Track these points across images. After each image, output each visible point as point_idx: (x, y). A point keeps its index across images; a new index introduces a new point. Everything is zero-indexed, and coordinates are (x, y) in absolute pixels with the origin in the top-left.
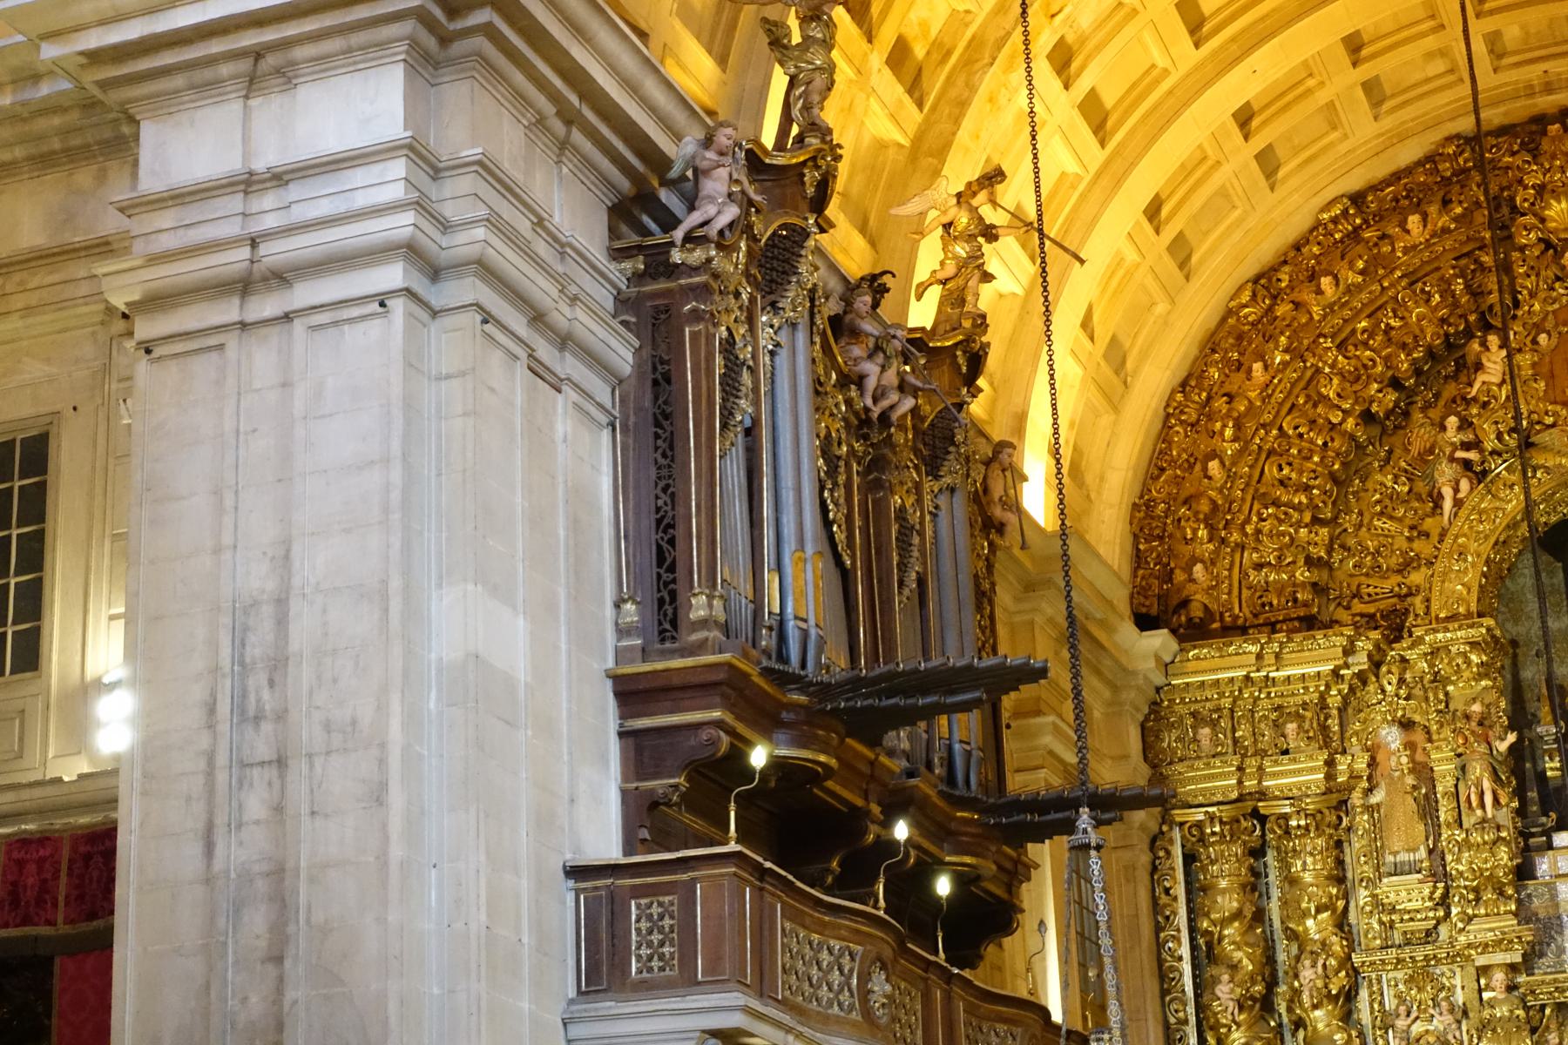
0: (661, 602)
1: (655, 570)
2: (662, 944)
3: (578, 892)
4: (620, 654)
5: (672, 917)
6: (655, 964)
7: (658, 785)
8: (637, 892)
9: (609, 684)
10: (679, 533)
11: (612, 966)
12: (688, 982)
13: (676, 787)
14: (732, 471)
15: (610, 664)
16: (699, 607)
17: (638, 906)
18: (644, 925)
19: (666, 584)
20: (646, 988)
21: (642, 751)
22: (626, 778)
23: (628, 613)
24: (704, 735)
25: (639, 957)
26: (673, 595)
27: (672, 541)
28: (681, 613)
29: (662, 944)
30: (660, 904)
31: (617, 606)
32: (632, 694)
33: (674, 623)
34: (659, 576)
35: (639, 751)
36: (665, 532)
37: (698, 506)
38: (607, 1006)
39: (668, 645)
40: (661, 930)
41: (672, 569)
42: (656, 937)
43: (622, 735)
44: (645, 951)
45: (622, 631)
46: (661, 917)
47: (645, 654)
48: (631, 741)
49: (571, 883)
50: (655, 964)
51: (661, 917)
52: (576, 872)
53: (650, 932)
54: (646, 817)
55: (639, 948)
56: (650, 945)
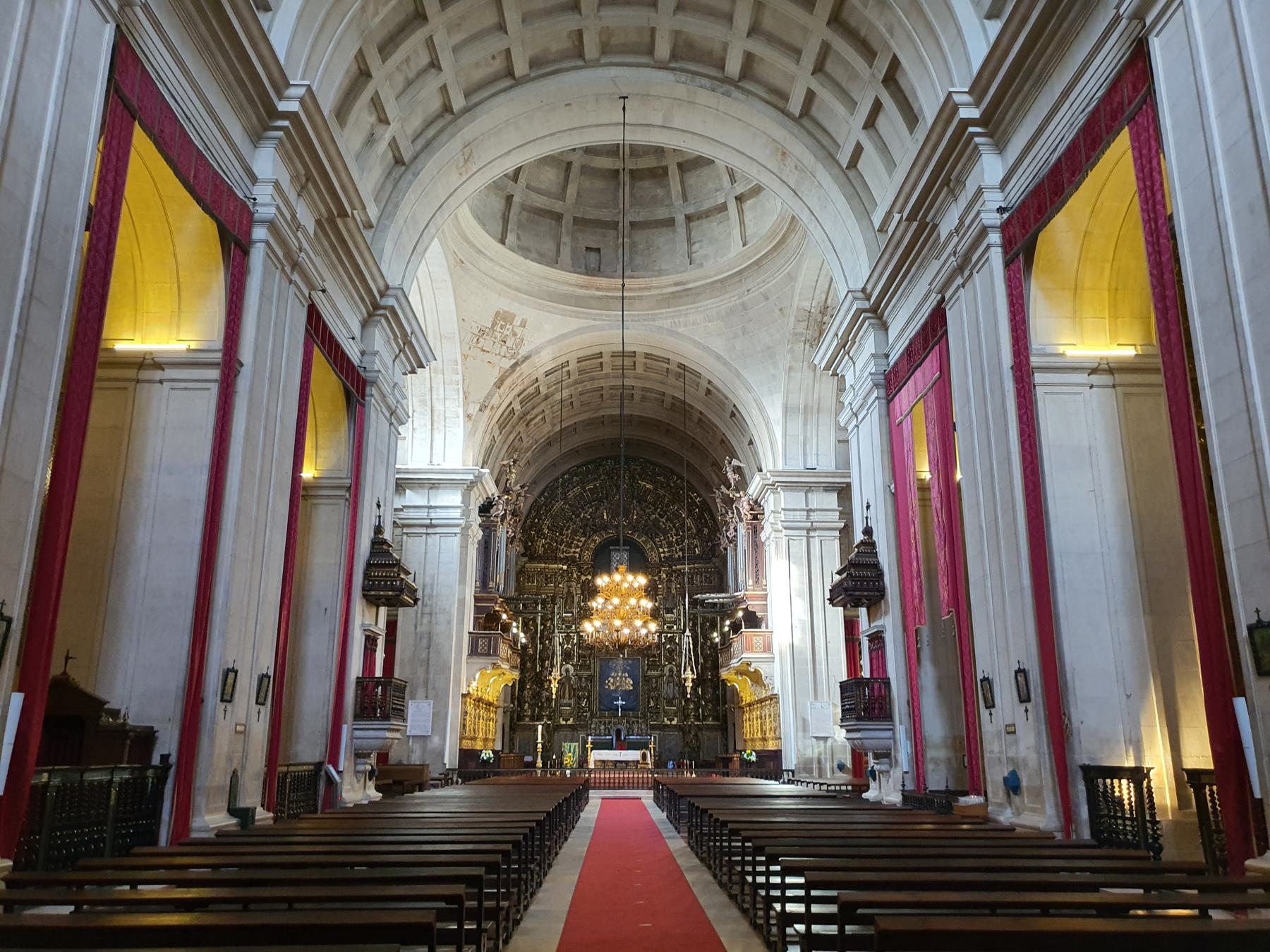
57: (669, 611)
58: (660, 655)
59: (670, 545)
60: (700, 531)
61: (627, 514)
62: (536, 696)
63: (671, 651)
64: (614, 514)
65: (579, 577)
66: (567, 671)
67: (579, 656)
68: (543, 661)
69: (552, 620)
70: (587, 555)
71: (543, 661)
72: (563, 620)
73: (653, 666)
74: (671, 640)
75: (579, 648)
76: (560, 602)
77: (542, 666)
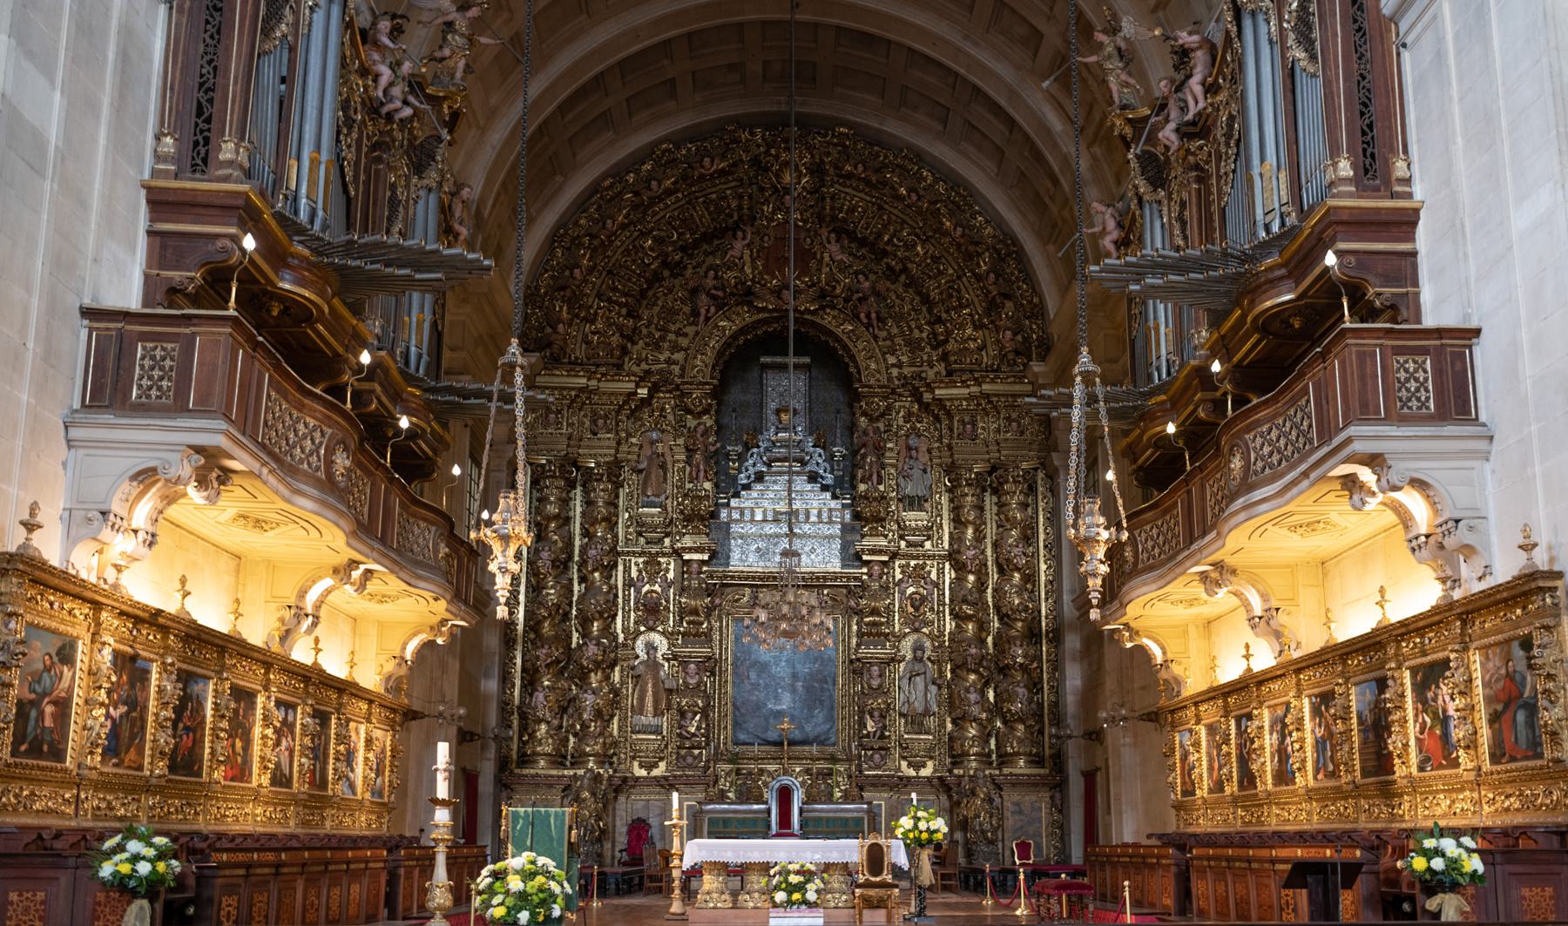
0: (196, 144)
1: (194, 119)
2: (161, 379)
3: (91, 330)
4: (155, 173)
5: (172, 359)
6: (154, 393)
7: (177, 275)
8: (144, 337)
9: (143, 192)
10: (217, 96)
11: (115, 388)
12: (179, 407)
13: (192, 279)
14: (270, 71)
15: (147, 176)
16: (227, 150)
17: (144, 348)
18: (147, 363)
19: (202, 131)
20: (143, 409)
21: (164, 248)
22: (149, 265)
23: (167, 145)
24: (220, 243)
25: (140, 387)
26: (207, 141)
27: (211, 101)
28: (211, 154)
29: (161, 379)
30: (163, 349)
31: (158, 138)
32: (161, 203)
33: (205, 161)
34: (197, 124)
35: (163, 247)
36: (206, 92)
37: (236, 78)
38: (109, 418)
39: (198, 175)
40: (162, 368)
41: (208, 121)
42: (156, 373)
43: (150, 233)
44: (145, 382)
45: (158, 157)
46: (163, 359)
47: (176, 177)
48: (158, 240)
49: (86, 322)
50: (154, 393)
51: (163, 359)
52: (88, 313)
53: (152, 368)
54: (160, 290)
55: (141, 378)
56: (150, 378)
57: (914, 503)
58: (889, 610)
59: (914, 346)
60: (992, 307)
61: (805, 258)
62: (567, 706)
63: (918, 602)
64: (773, 260)
65: (681, 422)
66: (651, 647)
67: (682, 612)
68: (585, 622)
69: (611, 524)
70: (702, 364)
71: (585, 622)
72: (641, 526)
73: (874, 634)
74: (918, 575)
75: (683, 590)
76: (631, 480)
77: (585, 634)
